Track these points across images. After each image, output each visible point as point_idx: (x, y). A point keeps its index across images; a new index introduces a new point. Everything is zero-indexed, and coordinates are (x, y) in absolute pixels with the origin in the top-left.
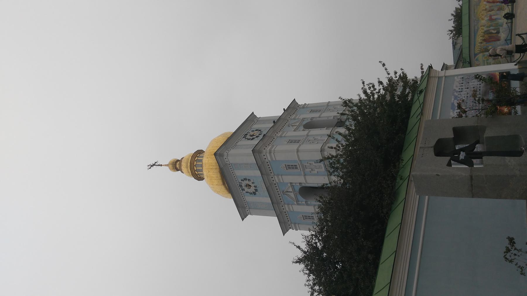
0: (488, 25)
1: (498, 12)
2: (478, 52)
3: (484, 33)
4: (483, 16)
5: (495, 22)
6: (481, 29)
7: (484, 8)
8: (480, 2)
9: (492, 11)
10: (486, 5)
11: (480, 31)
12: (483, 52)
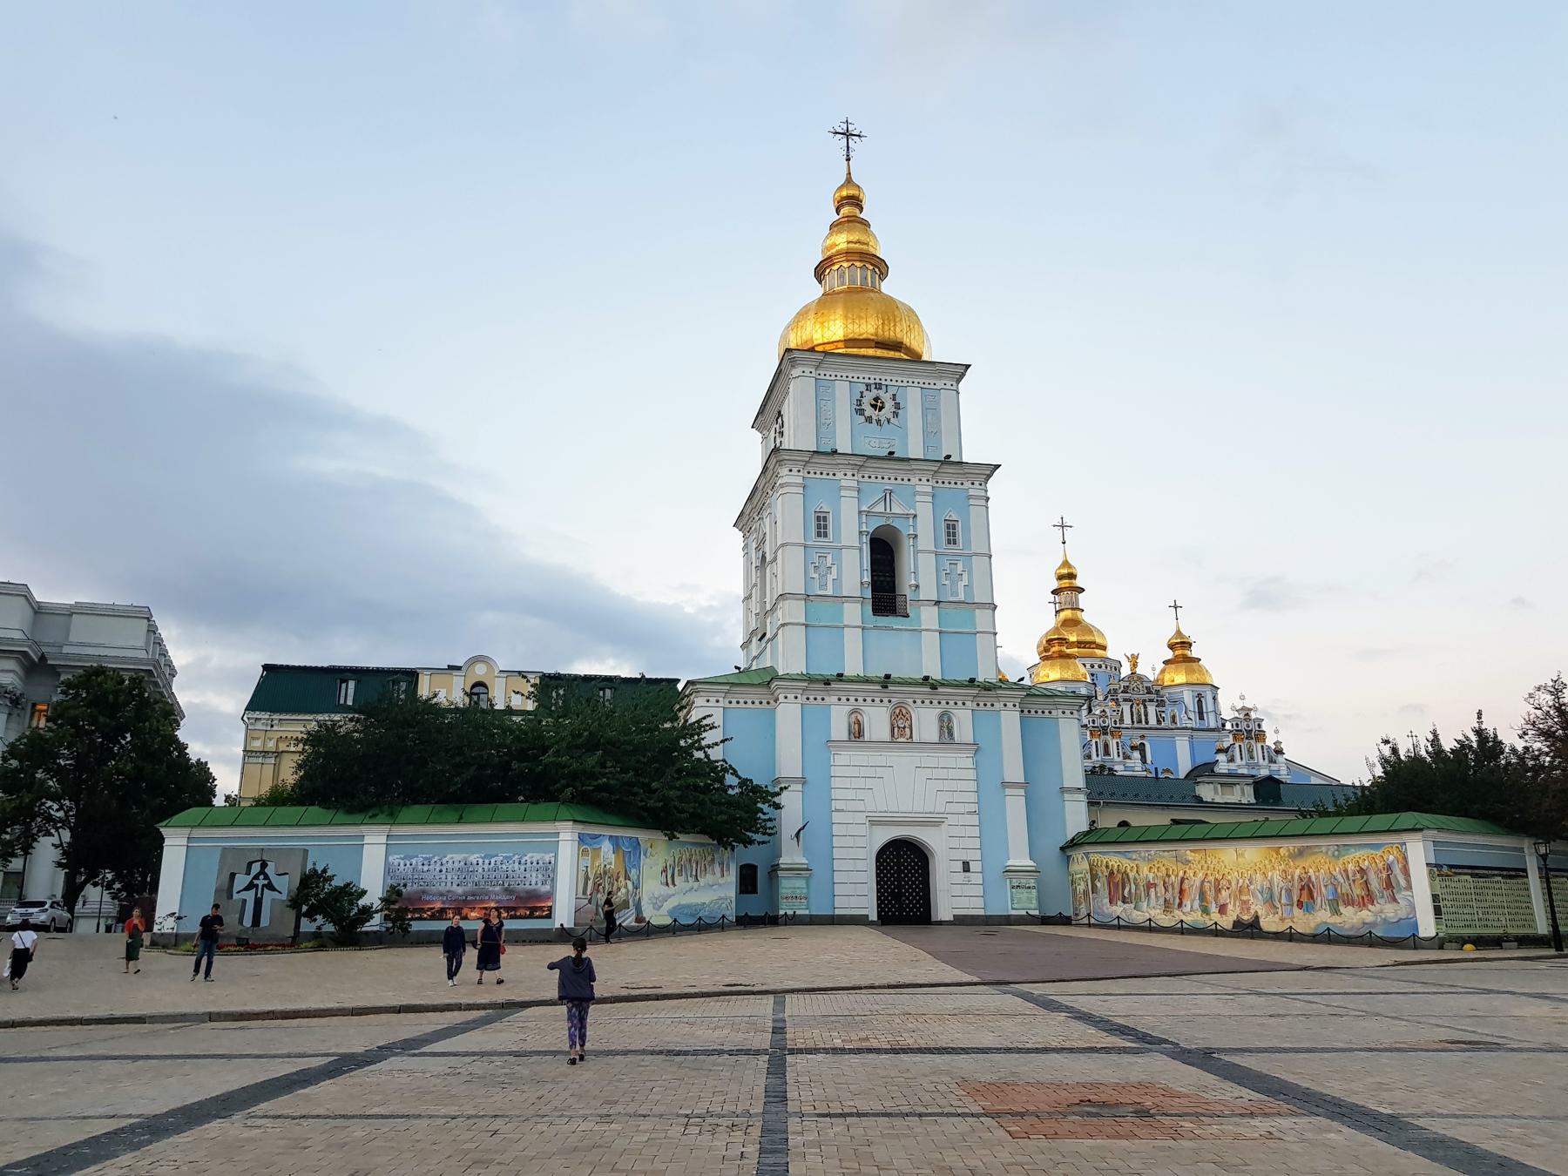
1: (1162, 901)
3: (1125, 872)
12: (1091, 870)
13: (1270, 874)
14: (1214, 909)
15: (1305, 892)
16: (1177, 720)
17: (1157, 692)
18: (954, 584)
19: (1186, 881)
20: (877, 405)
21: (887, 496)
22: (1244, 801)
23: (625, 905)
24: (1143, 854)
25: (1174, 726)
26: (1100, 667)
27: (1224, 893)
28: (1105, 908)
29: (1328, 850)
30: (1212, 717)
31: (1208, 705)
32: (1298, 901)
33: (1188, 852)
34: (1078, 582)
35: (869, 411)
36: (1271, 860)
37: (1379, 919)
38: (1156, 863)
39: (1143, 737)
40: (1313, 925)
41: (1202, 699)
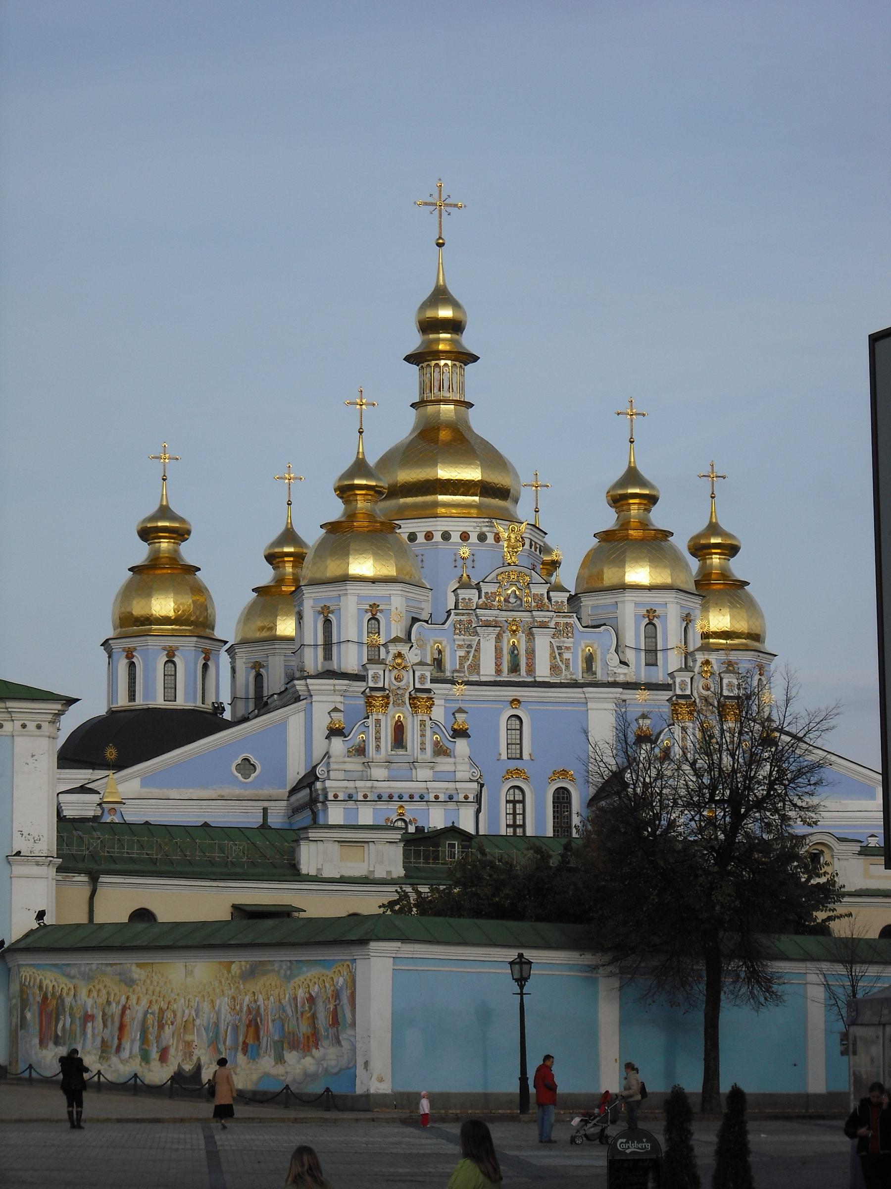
0: (75, 1009)
1: (98, 1041)
2: (22, 976)
4: (95, 994)
5: (78, 1029)
6: (69, 989)
7: (112, 996)
8: (126, 984)
9: (103, 1022)
10: (118, 1003)
11: (66, 984)
12: (22, 991)
13: (218, 1002)
14: (155, 1054)
15: (252, 1030)
16: (598, 667)
19: (128, 1012)
22: (380, 874)
24: (83, 969)
25: (590, 678)
26: (482, 537)
27: (168, 1031)
28: (33, 1053)
29: (281, 967)
32: (244, 1043)
33: (134, 968)
34: (469, 341)
36: (221, 982)
37: (320, 1070)
38: (96, 981)
39: (515, 702)
40: (255, 1077)
41: (656, 621)
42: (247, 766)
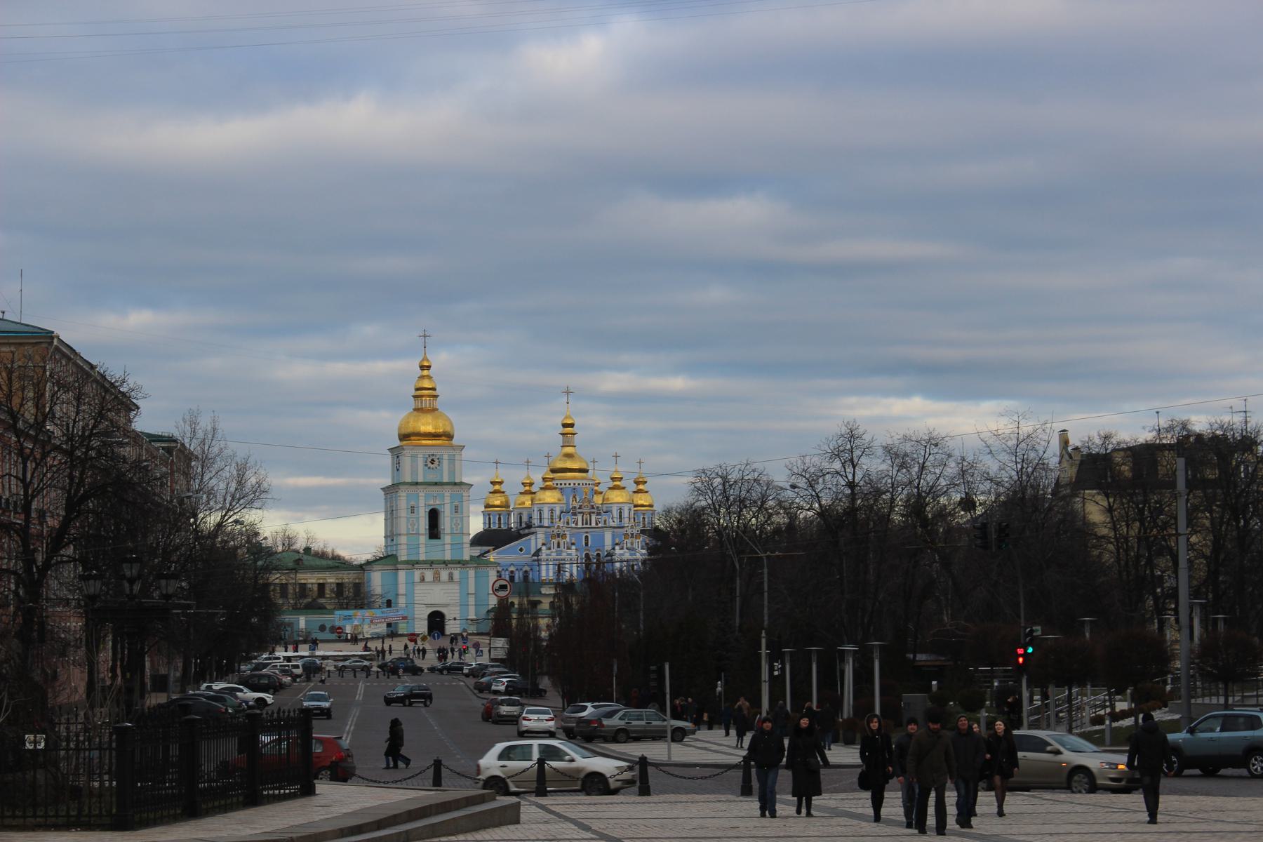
16: (607, 522)
17: (598, 507)
18: (457, 527)
20: (432, 461)
21: (435, 498)
23: (360, 633)
30: (627, 520)
31: (626, 514)
35: (430, 465)
39: (587, 532)
42: (521, 550)
